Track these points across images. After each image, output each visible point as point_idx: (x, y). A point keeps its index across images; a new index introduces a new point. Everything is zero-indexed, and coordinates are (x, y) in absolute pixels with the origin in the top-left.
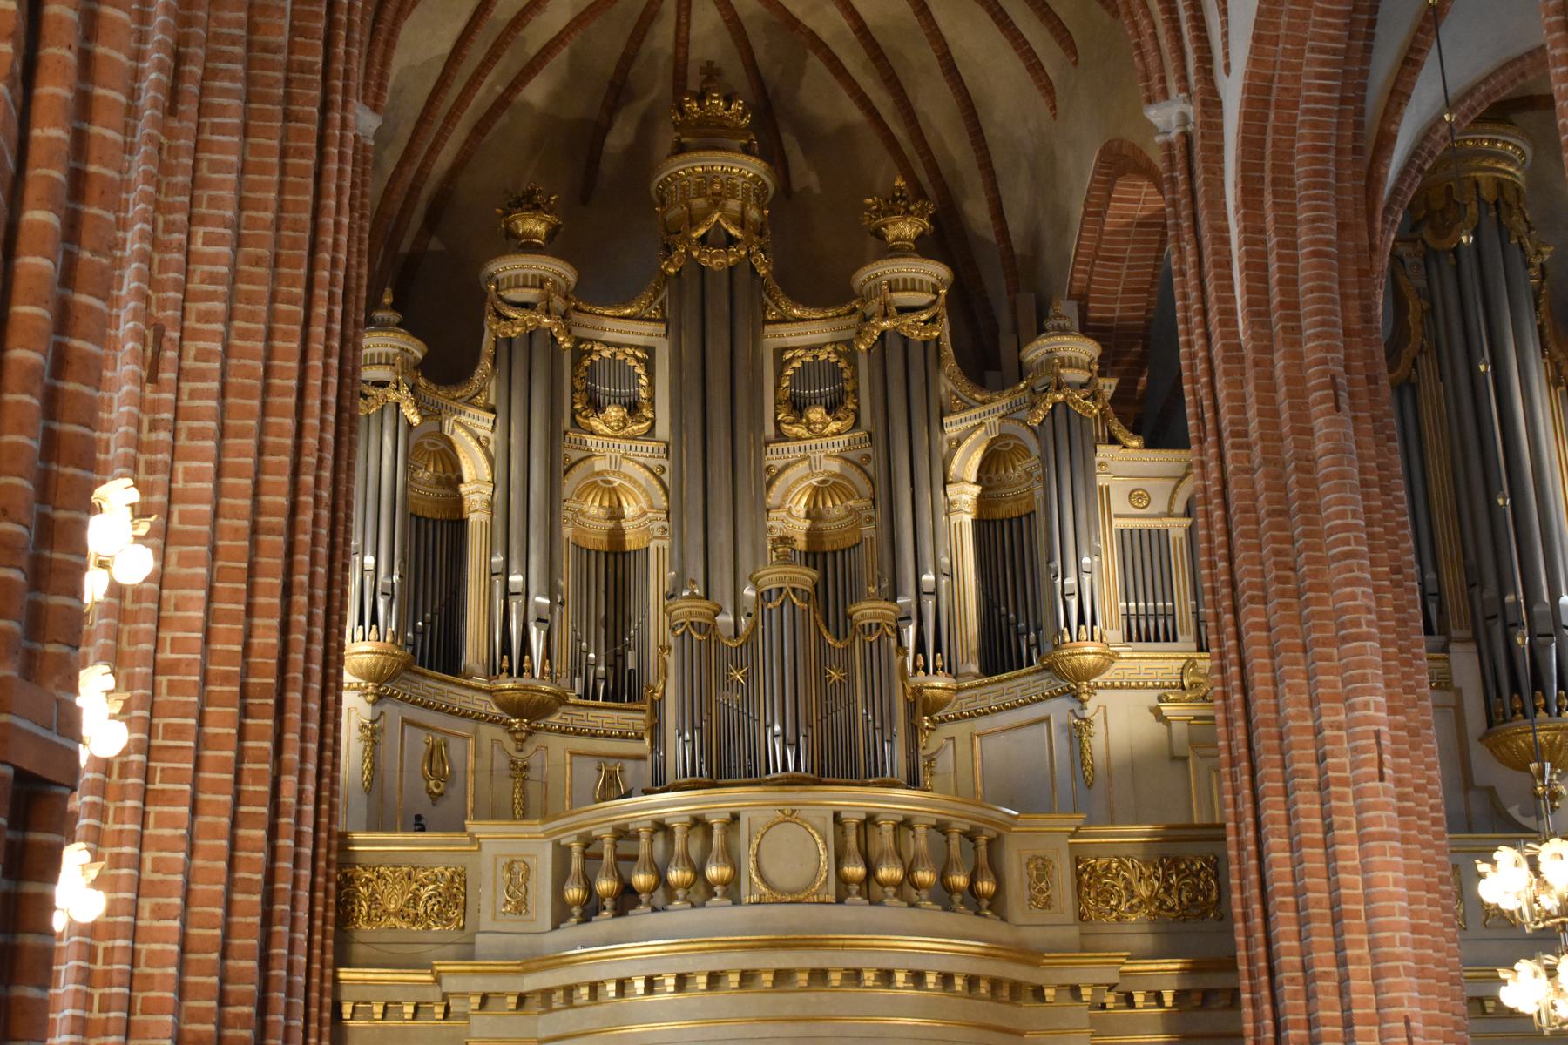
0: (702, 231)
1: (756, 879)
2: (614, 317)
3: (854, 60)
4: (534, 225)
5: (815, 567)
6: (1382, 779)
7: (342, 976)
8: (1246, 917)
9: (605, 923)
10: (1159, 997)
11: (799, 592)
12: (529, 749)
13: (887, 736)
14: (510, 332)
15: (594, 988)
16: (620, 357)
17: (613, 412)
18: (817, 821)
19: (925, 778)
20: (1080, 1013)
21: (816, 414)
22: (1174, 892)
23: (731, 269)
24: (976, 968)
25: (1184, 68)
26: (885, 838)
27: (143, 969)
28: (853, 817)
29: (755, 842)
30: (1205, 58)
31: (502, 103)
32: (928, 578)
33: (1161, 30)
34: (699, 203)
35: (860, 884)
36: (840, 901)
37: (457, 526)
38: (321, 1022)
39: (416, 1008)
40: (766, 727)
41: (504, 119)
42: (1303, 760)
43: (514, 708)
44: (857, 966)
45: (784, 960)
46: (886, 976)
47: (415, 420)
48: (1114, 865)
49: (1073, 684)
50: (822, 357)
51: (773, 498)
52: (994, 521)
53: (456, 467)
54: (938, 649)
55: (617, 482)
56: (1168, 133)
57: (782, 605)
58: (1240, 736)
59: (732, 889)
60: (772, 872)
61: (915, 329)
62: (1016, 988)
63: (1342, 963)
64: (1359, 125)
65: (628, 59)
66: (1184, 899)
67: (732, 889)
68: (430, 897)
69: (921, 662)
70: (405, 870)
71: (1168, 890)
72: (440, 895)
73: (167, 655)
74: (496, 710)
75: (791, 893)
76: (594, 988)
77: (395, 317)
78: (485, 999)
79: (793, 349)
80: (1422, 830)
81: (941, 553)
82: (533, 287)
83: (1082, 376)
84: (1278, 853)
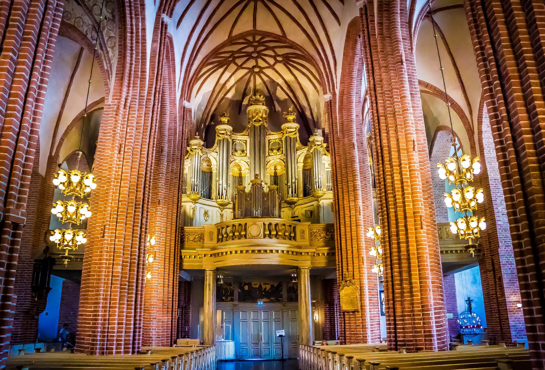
0: (254, 119)
3: (285, 87)
4: (225, 120)
6: (360, 215)
10: (324, 254)
15: (222, 253)
17: (239, 152)
19: (282, 216)
20: (309, 257)
21: (275, 151)
23: (260, 126)
27: (116, 250)
28: (267, 223)
30: (333, 86)
31: (223, 98)
32: (294, 180)
33: (326, 81)
34: (254, 114)
36: (264, 237)
37: (211, 173)
38: (177, 259)
39: (195, 257)
41: (224, 101)
42: (347, 212)
43: (221, 205)
47: (202, 155)
49: (317, 198)
51: (268, 166)
53: (211, 163)
54: (295, 193)
55: (240, 164)
58: (337, 208)
59: (245, 236)
61: (292, 136)
62: (297, 253)
63: (352, 248)
64: (360, 97)
65: (245, 89)
67: (245, 236)
71: (327, 235)
73: (121, 199)
77: (198, 137)
78: (205, 255)
80: (368, 224)
81: (296, 175)
83: (319, 143)
84: (343, 229)
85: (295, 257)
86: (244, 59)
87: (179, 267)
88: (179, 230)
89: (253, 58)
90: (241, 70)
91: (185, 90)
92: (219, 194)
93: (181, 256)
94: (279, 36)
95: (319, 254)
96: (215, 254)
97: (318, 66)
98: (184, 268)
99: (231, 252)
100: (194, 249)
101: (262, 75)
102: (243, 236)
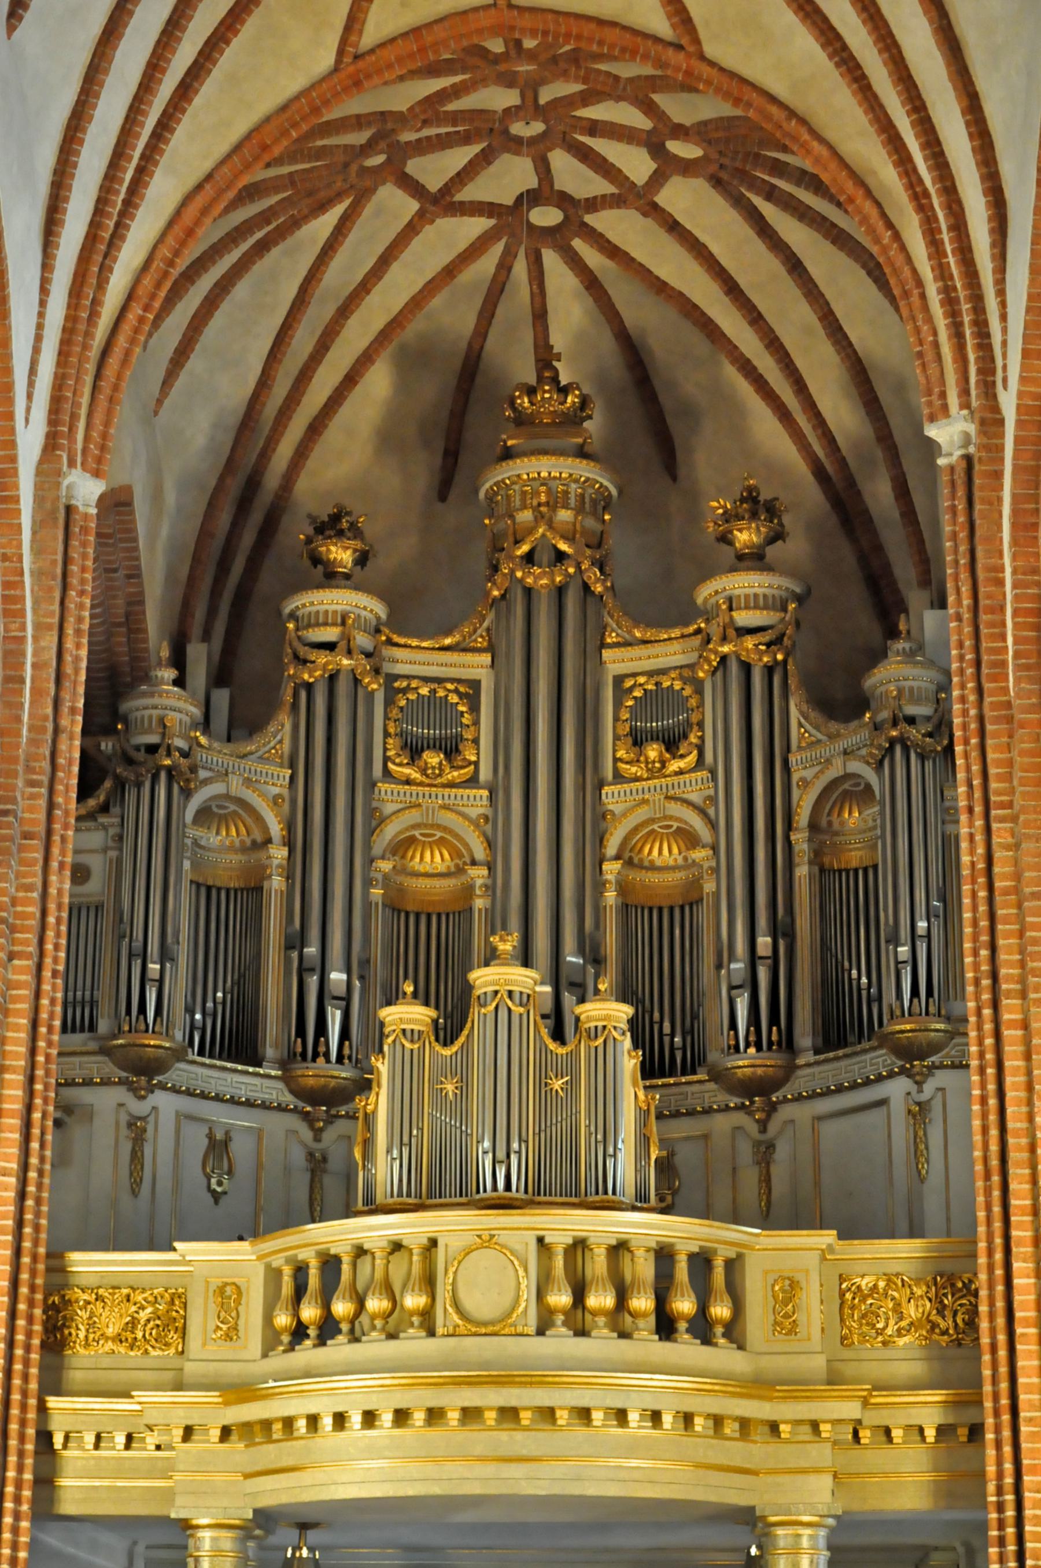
0: (525, 548)
1: (450, 1310)
2: (433, 649)
5: (427, 1004)
7: (50, 1405)
8: (994, 1348)
9: (307, 1354)
11: (409, 1034)
12: (330, 1135)
13: (611, 1150)
14: (306, 676)
15: (288, 1423)
16: (441, 693)
18: (518, 1247)
21: (653, 751)
22: (947, 1313)
23: (560, 591)
24: (689, 1404)
25: (966, 380)
26: (598, 1264)
28: (559, 1240)
29: (452, 1270)
30: (987, 368)
35: (566, 1313)
36: (541, 1332)
40: (478, 1142)
43: (313, 1096)
44: (547, 1403)
45: (471, 1397)
46: (584, 1414)
48: (882, 1284)
50: (666, 684)
52: (847, 871)
54: (774, 1019)
56: (951, 455)
57: (497, 1008)
58: (994, 1147)
60: (468, 1303)
62: (745, 1424)
66: (959, 1321)
68: (148, 1321)
69: (752, 1038)
70: (125, 1291)
71: (941, 1312)
72: (159, 1318)
74: (288, 1099)
75: (485, 1324)
76: (313, 1421)
79: (634, 675)
82: (334, 624)
85: (736, 1452)
86: (459, 157)
87: (34, 1501)
88: (33, 1273)
89: (516, 145)
90: (445, 224)
91: (76, 405)
92: (301, 1032)
93: (45, 1437)
94: (657, 40)
95: (888, 1431)
96: (247, 1429)
97: (897, 236)
98: (68, 1507)
99: (340, 1420)
100: (127, 1395)
101: (578, 244)
102: (416, 1320)
